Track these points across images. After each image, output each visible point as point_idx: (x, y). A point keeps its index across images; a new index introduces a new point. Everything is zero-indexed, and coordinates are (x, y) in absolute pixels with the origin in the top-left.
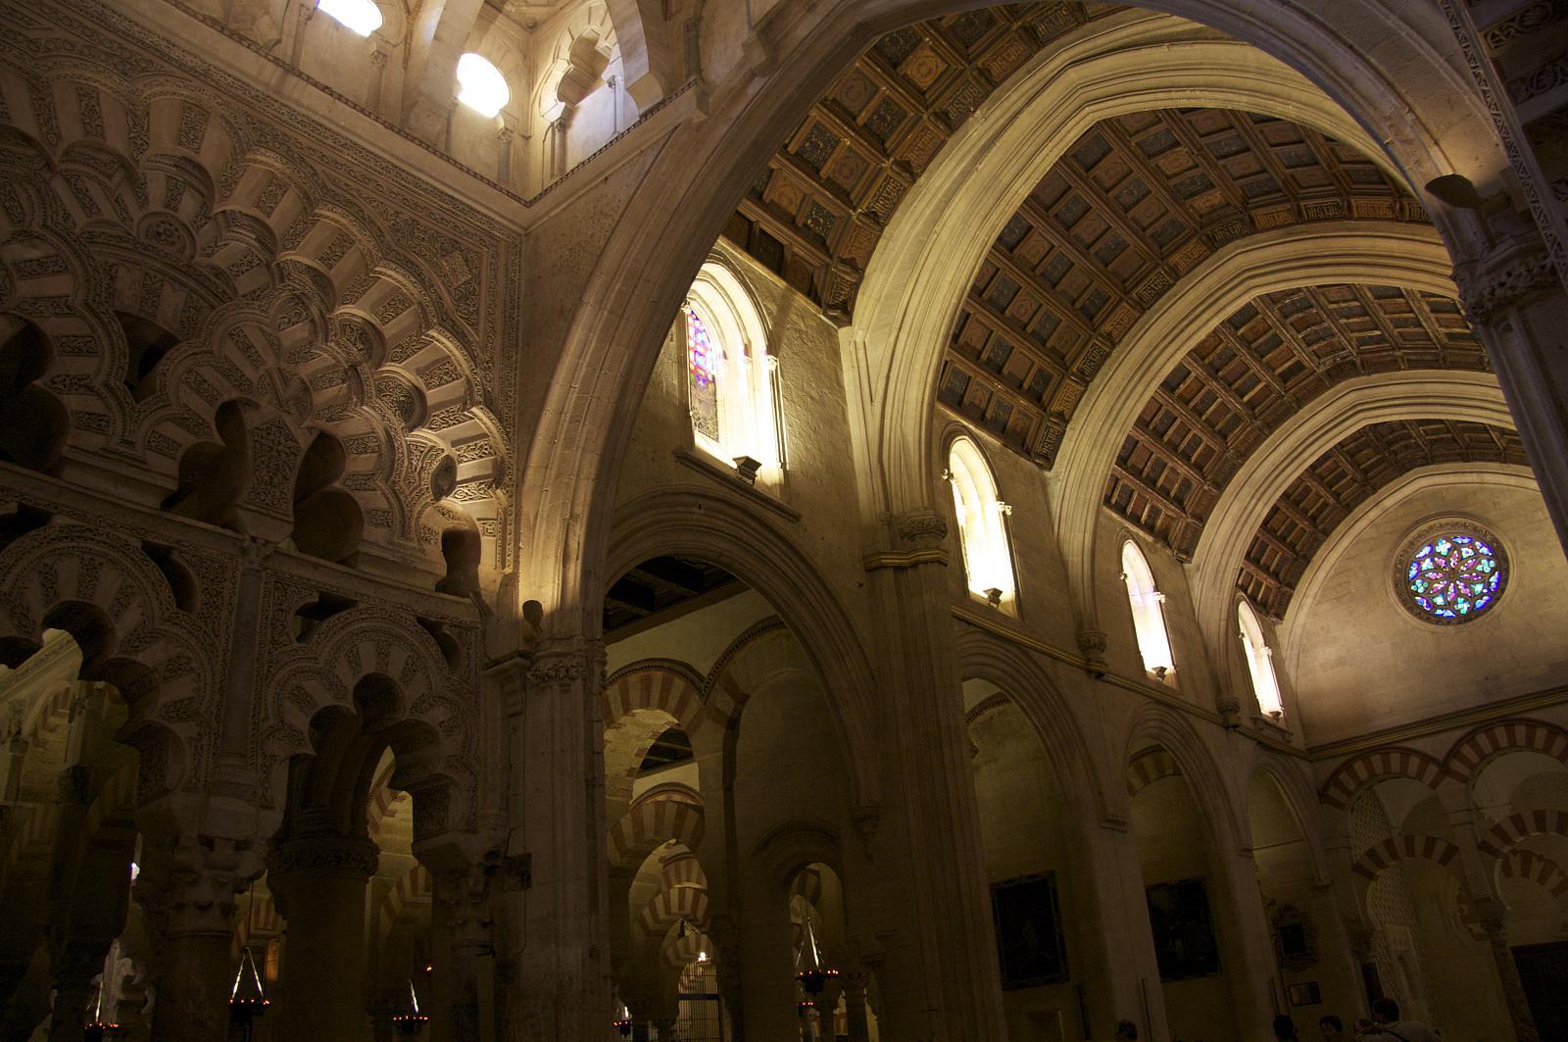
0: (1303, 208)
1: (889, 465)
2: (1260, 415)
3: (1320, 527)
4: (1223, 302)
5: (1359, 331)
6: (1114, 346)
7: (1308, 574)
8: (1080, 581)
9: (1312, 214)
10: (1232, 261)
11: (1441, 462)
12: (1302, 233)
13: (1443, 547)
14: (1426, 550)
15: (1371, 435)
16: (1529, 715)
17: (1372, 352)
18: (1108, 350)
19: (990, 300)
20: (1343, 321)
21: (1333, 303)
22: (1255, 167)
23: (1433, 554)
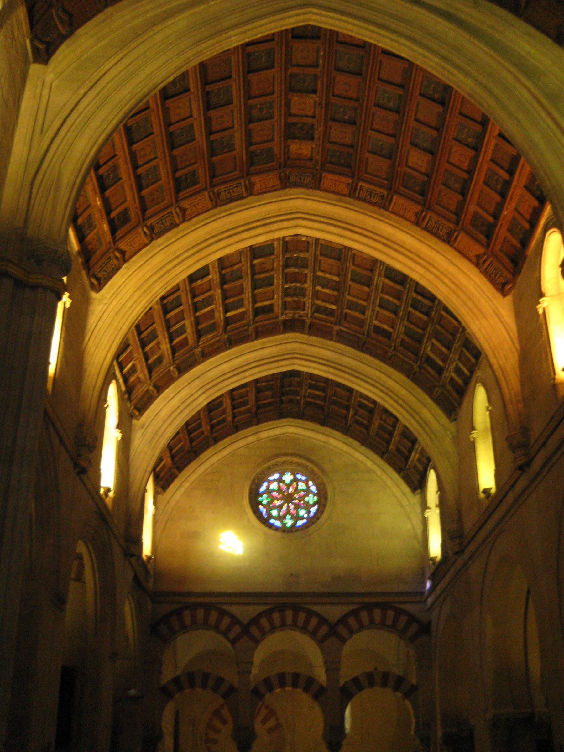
0: (359, 187)
1: (40, 187)
2: (230, 331)
3: (214, 435)
4: (275, 226)
5: (323, 301)
6: (184, 221)
7: (193, 465)
8: (91, 389)
9: (363, 194)
10: (294, 200)
11: (307, 420)
12: (350, 204)
13: (288, 478)
14: (276, 476)
15: (279, 381)
16: (310, 607)
17: (321, 320)
18: (178, 221)
19: (208, 93)
20: (319, 288)
21: (322, 271)
22: (348, 141)
23: (280, 480)
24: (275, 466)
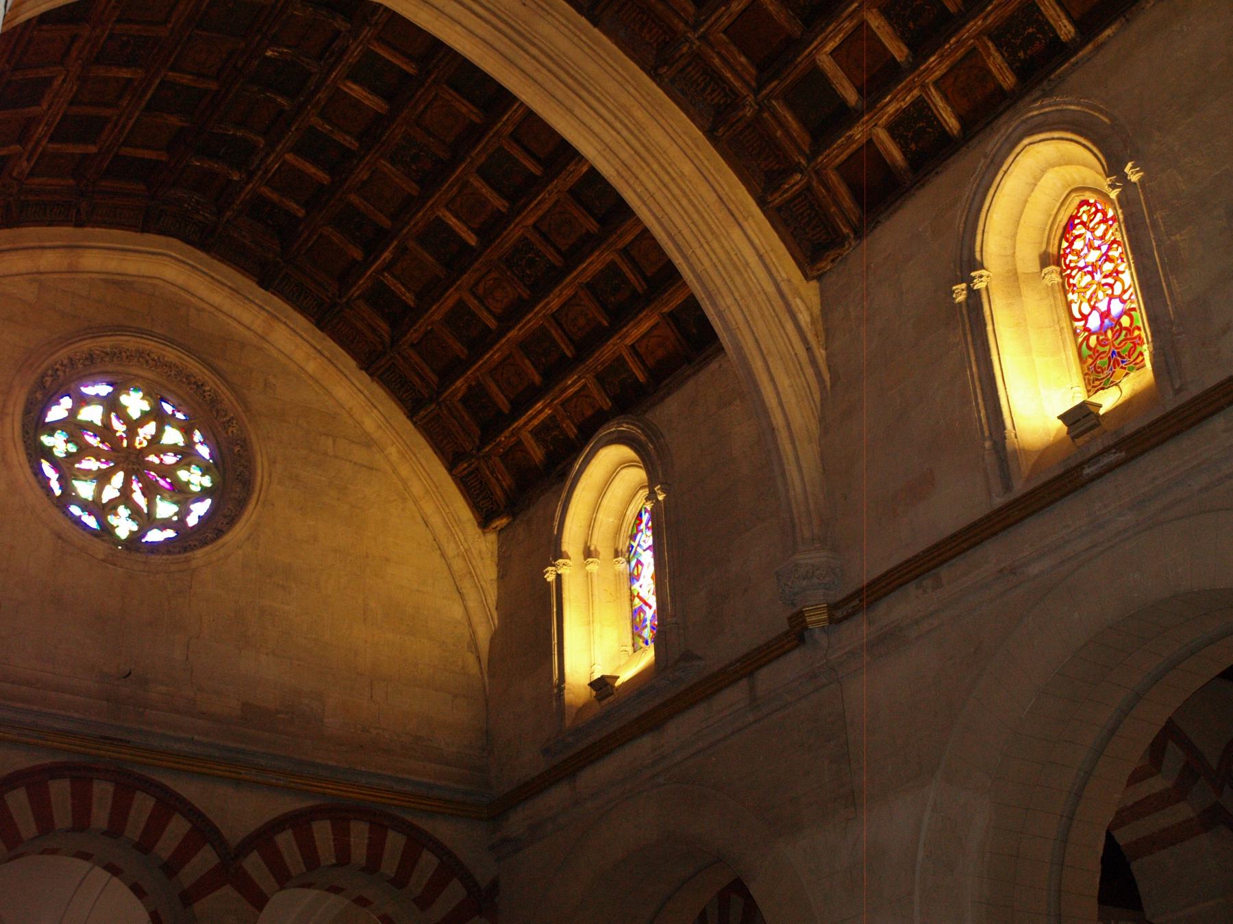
24: (107, 359)
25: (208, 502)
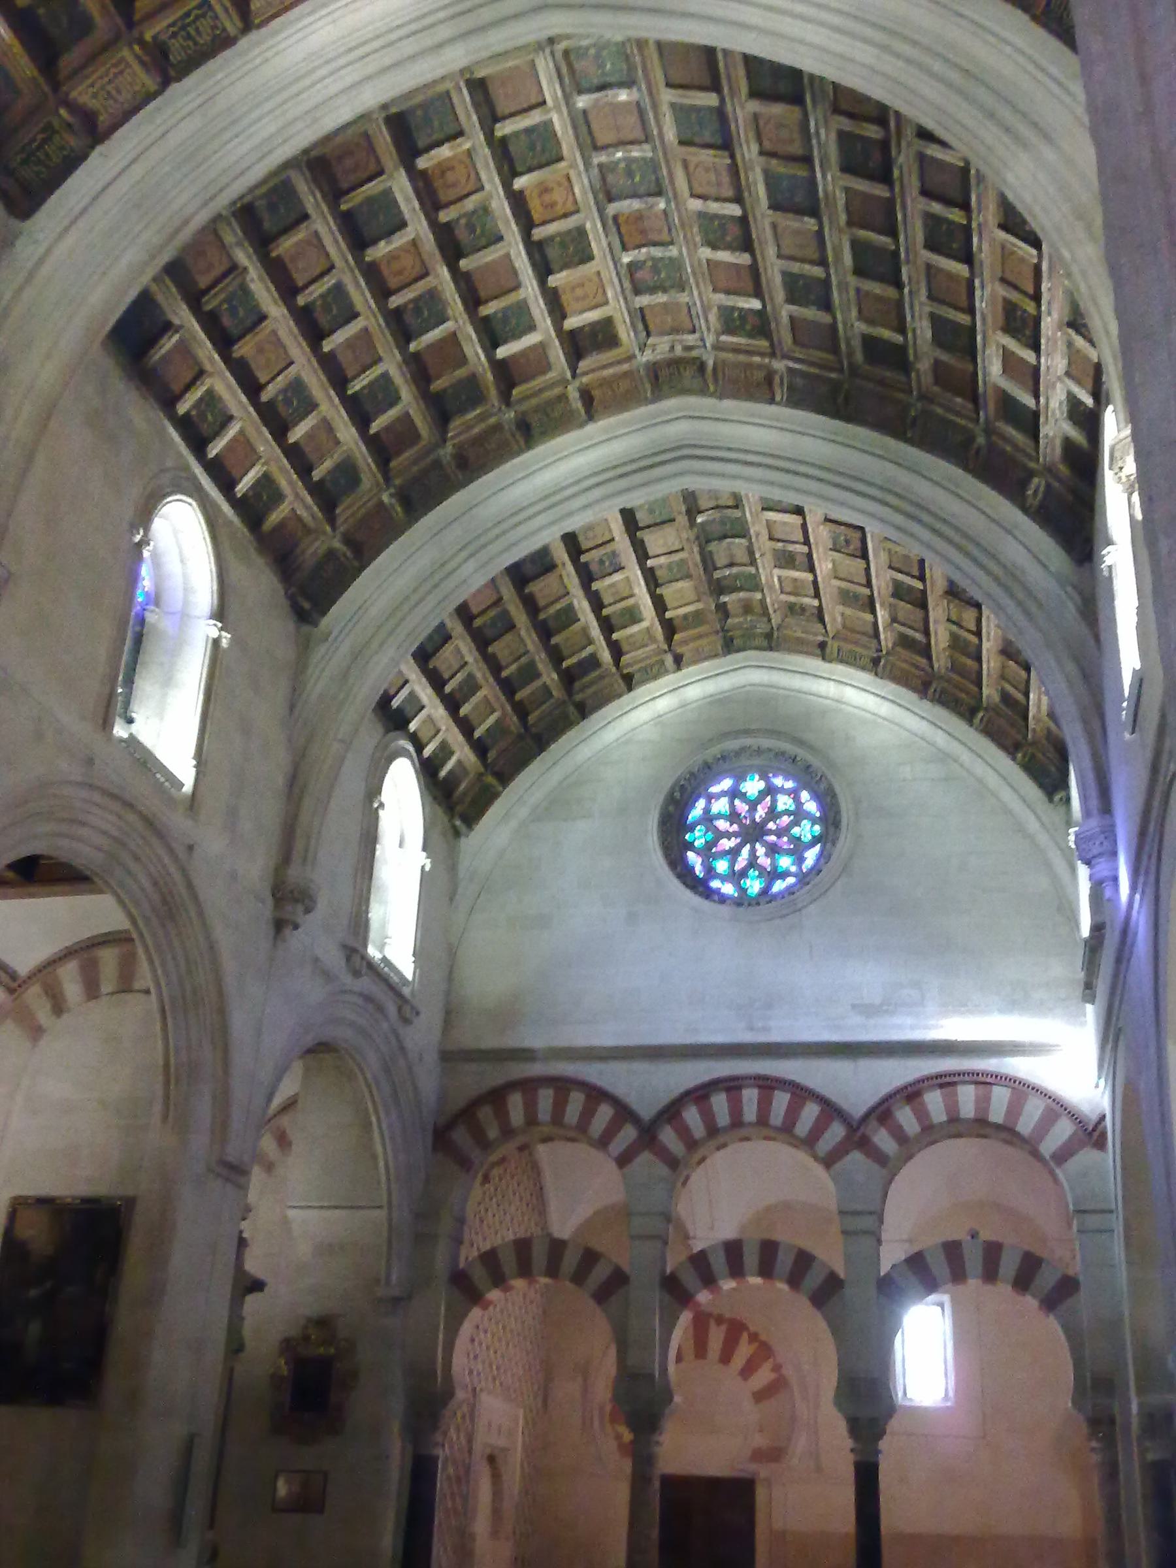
13: (753, 786)
14: (726, 784)
23: (734, 793)
25: (818, 847)
